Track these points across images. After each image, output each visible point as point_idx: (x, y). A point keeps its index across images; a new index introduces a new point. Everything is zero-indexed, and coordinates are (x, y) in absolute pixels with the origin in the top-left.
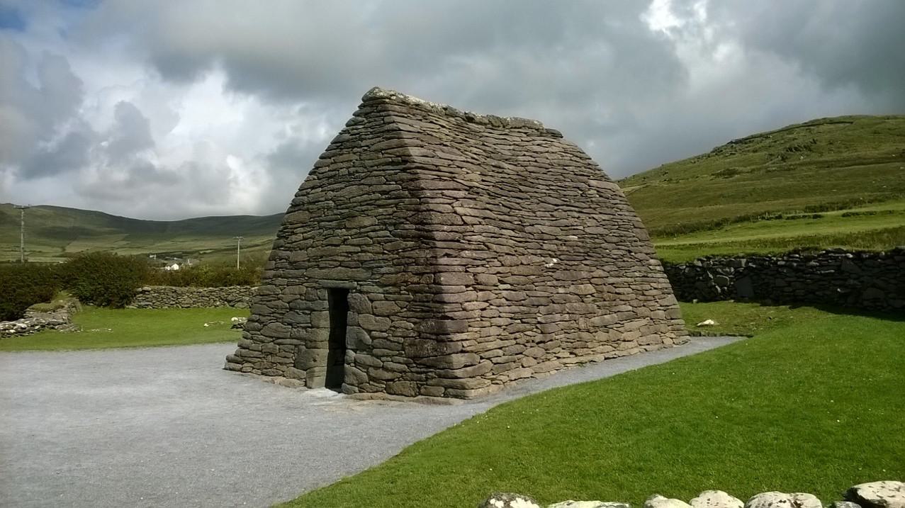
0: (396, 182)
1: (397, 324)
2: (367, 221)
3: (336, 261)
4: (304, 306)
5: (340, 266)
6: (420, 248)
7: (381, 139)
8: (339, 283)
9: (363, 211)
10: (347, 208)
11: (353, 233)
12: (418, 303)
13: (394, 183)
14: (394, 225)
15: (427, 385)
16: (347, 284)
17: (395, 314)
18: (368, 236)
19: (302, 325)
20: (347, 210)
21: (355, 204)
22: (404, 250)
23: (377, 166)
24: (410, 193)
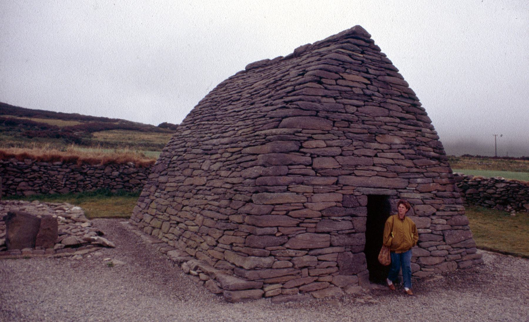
3: (373, 170)
5: (377, 175)
7: (382, 73)
8: (381, 191)
9: (389, 130)
10: (374, 125)
11: (385, 148)
12: (447, 205)
14: (418, 146)
15: (462, 261)
16: (390, 192)
17: (434, 214)
18: (399, 152)
19: (344, 232)
20: (374, 127)
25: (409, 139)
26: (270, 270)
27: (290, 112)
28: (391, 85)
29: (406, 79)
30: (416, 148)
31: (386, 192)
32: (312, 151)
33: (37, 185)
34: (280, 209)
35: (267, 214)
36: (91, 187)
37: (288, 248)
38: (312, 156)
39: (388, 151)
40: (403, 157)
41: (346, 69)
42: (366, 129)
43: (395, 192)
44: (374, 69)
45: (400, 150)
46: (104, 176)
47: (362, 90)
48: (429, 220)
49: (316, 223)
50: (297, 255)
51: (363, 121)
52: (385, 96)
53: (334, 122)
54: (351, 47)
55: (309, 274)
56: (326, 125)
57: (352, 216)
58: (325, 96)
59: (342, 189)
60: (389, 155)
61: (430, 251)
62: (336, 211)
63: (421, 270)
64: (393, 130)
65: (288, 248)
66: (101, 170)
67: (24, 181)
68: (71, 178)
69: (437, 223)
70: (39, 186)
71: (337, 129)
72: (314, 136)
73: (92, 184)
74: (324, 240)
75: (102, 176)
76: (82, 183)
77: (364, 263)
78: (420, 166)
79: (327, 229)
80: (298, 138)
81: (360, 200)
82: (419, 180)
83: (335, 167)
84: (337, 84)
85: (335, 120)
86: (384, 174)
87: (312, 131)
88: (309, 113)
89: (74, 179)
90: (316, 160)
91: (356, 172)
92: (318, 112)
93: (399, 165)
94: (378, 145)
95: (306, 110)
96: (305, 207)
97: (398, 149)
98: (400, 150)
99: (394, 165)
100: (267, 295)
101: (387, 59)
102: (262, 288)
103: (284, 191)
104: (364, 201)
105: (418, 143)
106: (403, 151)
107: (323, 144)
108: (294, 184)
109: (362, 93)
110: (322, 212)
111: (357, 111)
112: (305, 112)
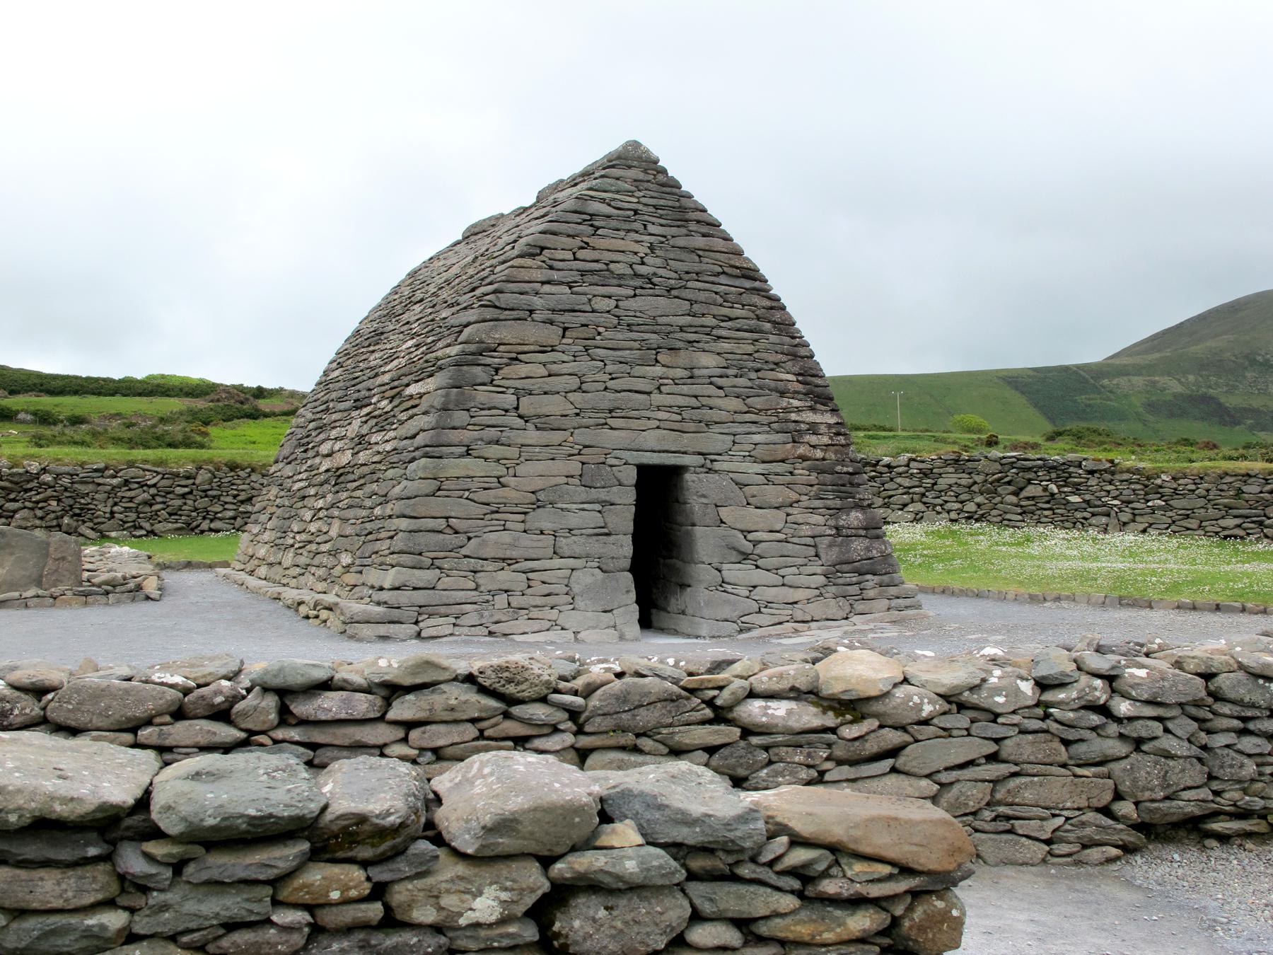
0: (743, 305)
1: (800, 518)
2: (708, 362)
3: (649, 419)
4: (584, 497)
6: (812, 409)
7: (683, 231)
9: (690, 342)
13: (740, 306)
14: (758, 371)
18: (711, 383)
19: (584, 531)
21: (669, 328)
22: (787, 410)
23: (697, 274)
24: (775, 327)
25: (738, 357)
26: (432, 591)
27: (471, 315)
28: (700, 253)
29: (739, 239)
30: (753, 375)
31: (678, 459)
32: (518, 384)
33: (52, 516)
34: (452, 487)
35: (427, 496)
36: (167, 516)
37: (465, 556)
38: (518, 393)
39: (689, 381)
40: (721, 393)
41: (598, 228)
42: (635, 341)
43: (700, 459)
44: (662, 225)
45: (713, 379)
46: (195, 492)
47: (631, 266)
48: (781, 514)
49: (525, 513)
50: (484, 569)
51: (628, 325)
52: (686, 277)
53: (565, 329)
54: (612, 185)
55: (509, 604)
56: (551, 335)
57: (604, 503)
58: (548, 282)
59: (579, 454)
60: (685, 389)
61: (783, 577)
62: (567, 493)
63: (760, 612)
64: (698, 342)
65: (465, 556)
66: (188, 478)
67: (25, 508)
68: (123, 497)
69: (801, 521)
70: (57, 518)
71: (570, 341)
72: (521, 357)
73: (169, 510)
74: (540, 544)
75: (191, 493)
76: (147, 509)
77: (628, 592)
78: (760, 411)
79: (547, 525)
80: (489, 361)
81: (618, 474)
82: (757, 438)
83: (564, 413)
84: (575, 259)
85: (566, 325)
86: (677, 425)
87: (520, 348)
88: (515, 314)
89: (131, 499)
90: (525, 401)
91: (611, 422)
92: (531, 312)
93: (711, 408)
94: (665, 369)
95: (506, 309)
96: (504, 486)
97: (710, 377)
98: (712, 379)
99: (698, 408)
100: (423, 634)
101: (696, 202)
102: (416, 623)
103: (461, 456)
104: (631, 475)
105: (759, 365)
106: (720, 381)
107: (542, 371)
108: (479, 443)
109: (629, 271)
110: (538, 494)
111: (617, 307)
112: (507, 312)
